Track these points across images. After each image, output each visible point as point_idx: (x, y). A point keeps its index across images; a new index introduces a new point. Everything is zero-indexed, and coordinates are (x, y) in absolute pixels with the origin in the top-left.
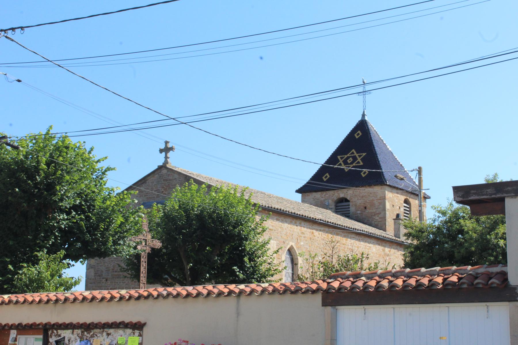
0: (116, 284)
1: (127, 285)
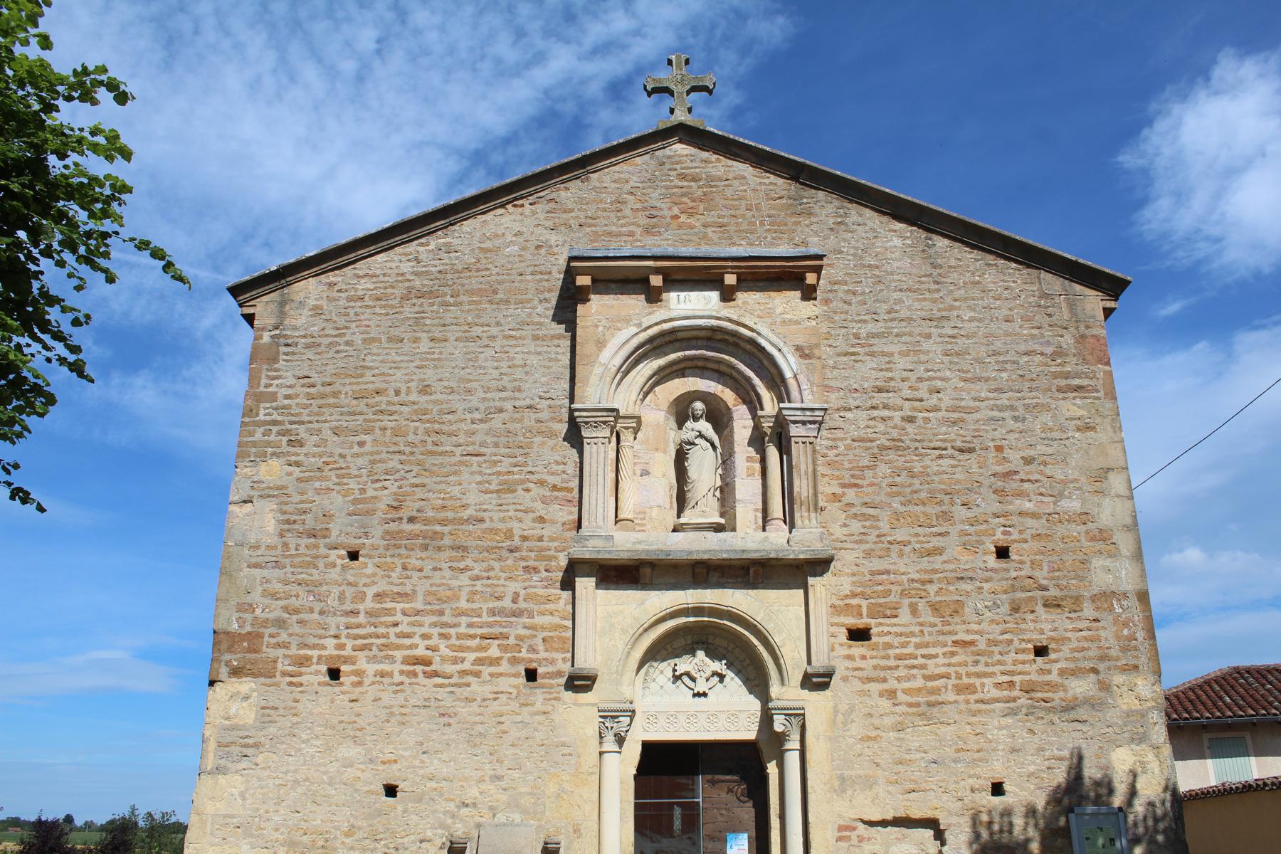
0: (416, 575)
1: (479, 583)
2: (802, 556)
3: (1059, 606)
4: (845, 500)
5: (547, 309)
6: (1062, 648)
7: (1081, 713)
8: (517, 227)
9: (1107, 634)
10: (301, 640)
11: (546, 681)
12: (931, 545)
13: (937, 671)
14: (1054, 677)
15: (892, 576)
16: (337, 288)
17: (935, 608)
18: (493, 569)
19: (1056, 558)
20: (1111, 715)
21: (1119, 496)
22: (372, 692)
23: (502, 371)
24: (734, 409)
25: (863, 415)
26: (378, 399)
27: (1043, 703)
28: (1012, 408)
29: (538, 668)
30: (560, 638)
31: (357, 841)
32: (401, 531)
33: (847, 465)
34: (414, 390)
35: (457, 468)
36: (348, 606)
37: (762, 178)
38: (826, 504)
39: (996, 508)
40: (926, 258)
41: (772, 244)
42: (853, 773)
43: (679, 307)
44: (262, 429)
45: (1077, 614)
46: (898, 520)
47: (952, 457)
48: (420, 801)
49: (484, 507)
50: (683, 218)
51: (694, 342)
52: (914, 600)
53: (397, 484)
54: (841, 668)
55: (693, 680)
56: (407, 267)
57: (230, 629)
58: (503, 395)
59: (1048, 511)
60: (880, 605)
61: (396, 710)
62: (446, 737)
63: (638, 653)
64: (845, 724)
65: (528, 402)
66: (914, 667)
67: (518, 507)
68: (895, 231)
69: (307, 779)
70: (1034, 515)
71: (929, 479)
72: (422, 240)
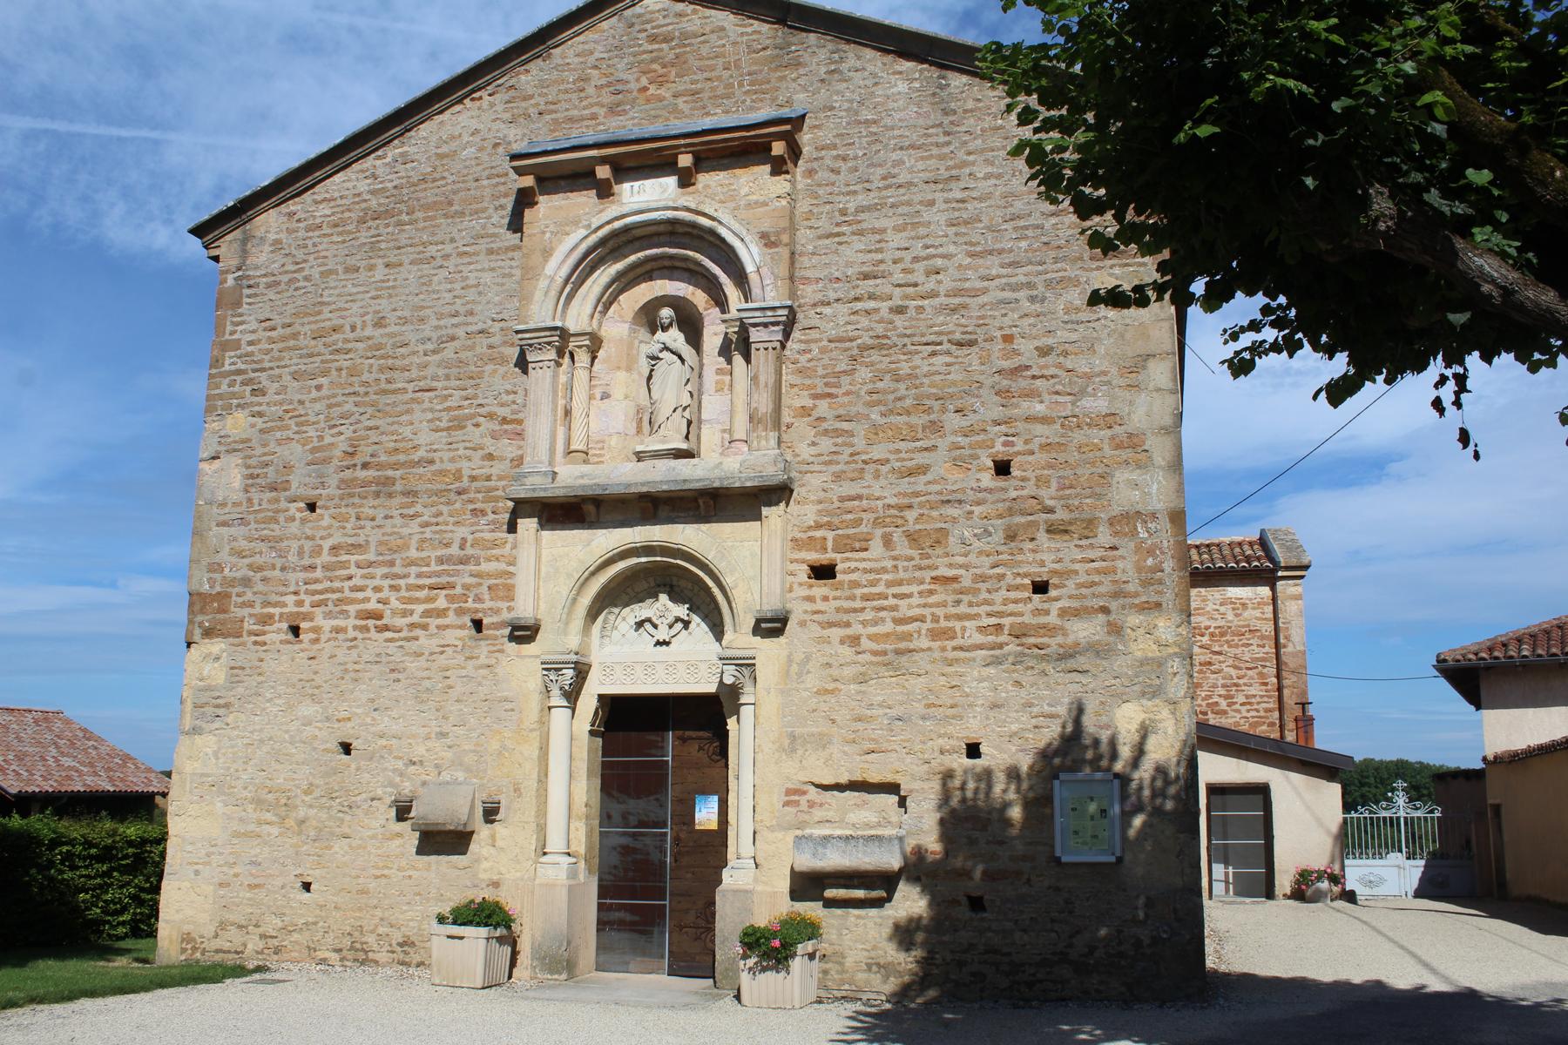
0: (369, 524)
2: (749, 484)
3: (1066, 531)
4: (815, 414)
5: (502, 217)
6: (1066, 582)
7: (1081, 662)
8: (474, 124)
9: (1126, 566)
10: (264, 598)
11: (491, 632)
12: (914, 462)
13: (910, 613)
14: (1052, 619)
15: (865, 502)
16: (296, 217)
17: (913, 538)
19: (1069, 472)
20: (1120, 664)
21: (1158, 390)
22: (328, 648)
23: (455, 293)
24: (705, 313)
25: (843, 309)
26: (335, 336)
27: (1036, 650)
28: (1030, 285)
32: (356, 479)
33: (820, 371)
34: (369, 323)
36: (307, 562)
37: (745, 26)
38: (793, 420)
39: (997, 412)
40: (937, 103)
41: (751, 109)
42: (805, 730)
43: (632, 200)
44: (227, 381)
45: (1090, 541)
46: (876, 434)
47: (948, 353)
48: (371, 759)
49: (435, 447)
50: (652, 90)
51: (656, 239)
52: (888, 530)
54: (798, 611)
55: (655, 626)
56: (363, 186)
57: (202, 591)
58: (455, 320)
59: (1064, 414)
60: (848, 536)
61: (351, 667)
63: (586, 600)
64: (800, 675)
65: (480, 326)
66: (883, 609)
67: (468, 445)
68: (901, 73)
69: (270, 739)
70: (1045, 420)
71: (918, 382)
72: (380, 153)
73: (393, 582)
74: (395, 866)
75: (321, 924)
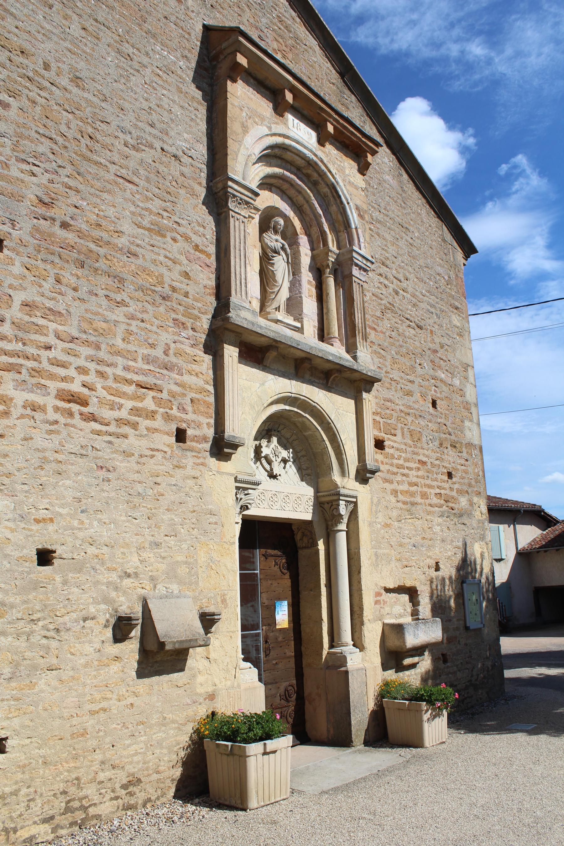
0: (71, 293)
1: (134, 323)
2: (369, 374)
11: (194, 444)
18: (146, 312)
24: (300, 236)
29: (188, 429)
30: (205, 402)
31: (9, 623)
32: (52, 235)
35: (110, 186)
53: (47, 176)
62: (105, 494)
67: (168, 254)
73: (99, 368)
74: (115, 697)
75: (24, 791)
